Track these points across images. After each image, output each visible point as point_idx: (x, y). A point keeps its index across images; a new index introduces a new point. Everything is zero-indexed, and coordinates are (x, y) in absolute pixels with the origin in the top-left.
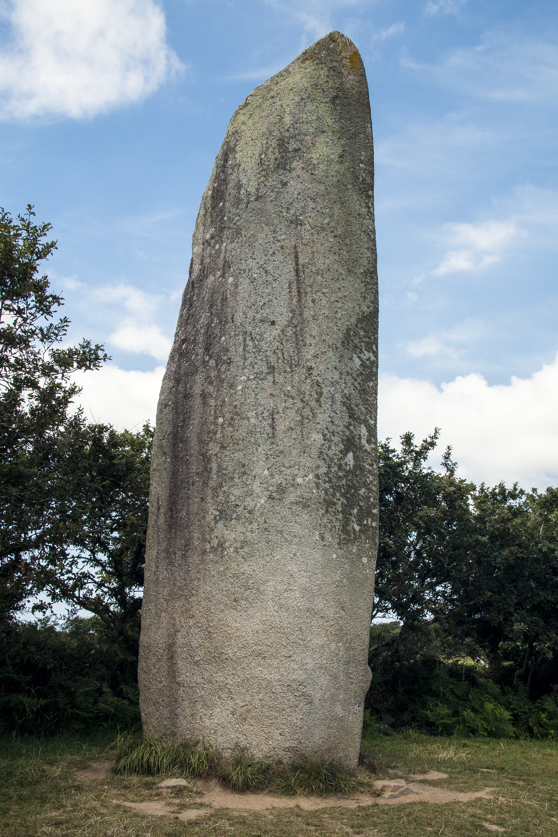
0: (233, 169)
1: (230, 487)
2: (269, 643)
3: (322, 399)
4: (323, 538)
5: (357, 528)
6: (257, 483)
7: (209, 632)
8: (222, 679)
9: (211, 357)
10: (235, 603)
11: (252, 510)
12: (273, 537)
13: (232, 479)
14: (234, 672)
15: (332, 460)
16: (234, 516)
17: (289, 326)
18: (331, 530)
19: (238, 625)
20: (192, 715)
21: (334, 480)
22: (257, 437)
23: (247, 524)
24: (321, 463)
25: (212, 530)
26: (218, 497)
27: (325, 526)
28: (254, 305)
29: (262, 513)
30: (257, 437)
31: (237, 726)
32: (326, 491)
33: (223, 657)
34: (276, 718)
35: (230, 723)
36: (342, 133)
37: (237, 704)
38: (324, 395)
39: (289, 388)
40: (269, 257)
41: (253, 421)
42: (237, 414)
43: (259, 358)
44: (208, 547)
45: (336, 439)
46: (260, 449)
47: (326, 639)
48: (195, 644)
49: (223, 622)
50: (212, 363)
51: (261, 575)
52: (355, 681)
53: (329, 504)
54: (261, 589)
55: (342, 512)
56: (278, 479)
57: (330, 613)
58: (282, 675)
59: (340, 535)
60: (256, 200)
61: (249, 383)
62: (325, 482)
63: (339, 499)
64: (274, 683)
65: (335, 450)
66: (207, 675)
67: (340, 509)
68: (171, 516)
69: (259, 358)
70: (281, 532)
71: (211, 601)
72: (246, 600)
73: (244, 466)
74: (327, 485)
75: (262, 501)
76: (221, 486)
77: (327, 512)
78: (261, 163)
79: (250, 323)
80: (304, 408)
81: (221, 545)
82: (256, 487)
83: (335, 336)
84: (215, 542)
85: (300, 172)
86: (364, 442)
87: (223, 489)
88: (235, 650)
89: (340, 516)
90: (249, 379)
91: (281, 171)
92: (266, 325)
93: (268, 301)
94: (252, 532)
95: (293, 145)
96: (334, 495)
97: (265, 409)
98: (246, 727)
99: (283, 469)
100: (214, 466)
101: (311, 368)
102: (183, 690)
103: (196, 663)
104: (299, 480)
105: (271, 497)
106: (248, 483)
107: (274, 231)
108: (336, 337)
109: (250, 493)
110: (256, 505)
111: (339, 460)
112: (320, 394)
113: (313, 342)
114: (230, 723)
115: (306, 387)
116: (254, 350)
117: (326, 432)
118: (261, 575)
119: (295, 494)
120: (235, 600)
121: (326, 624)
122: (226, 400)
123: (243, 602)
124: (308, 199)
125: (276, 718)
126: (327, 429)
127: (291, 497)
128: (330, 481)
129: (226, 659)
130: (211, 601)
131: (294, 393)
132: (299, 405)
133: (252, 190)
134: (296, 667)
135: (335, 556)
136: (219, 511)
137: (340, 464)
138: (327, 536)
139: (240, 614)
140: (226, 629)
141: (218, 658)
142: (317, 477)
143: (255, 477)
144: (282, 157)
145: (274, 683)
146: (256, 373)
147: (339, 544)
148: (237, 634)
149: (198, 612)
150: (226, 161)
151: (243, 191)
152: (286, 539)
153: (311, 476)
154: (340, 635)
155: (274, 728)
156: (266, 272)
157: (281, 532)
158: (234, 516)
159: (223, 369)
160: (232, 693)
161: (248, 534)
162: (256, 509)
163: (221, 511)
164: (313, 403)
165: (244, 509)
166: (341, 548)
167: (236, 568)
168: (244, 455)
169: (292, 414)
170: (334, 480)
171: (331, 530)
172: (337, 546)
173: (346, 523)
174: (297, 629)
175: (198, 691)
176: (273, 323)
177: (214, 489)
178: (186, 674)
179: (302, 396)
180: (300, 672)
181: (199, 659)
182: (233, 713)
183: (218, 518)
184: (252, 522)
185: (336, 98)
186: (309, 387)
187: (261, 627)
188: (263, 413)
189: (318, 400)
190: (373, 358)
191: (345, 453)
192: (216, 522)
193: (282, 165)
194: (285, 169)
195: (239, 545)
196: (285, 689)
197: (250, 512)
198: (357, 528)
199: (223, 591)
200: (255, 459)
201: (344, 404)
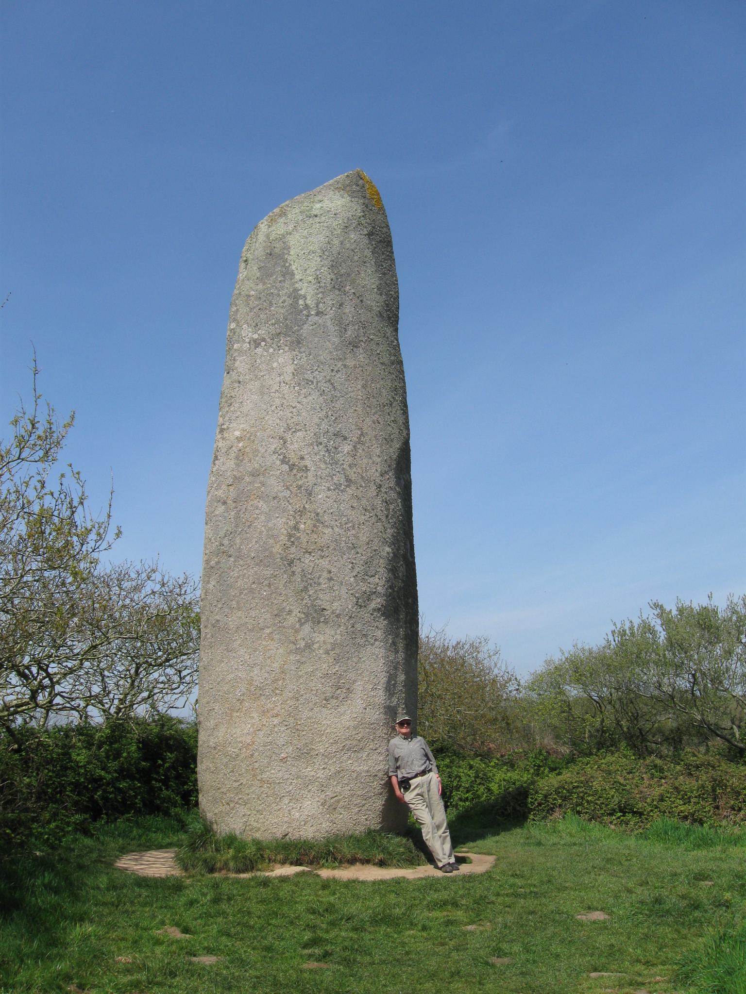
0: (284, 276)
8: (313, 773)
12: (362, 641)
33: (313, 753)
36: (378, 264)
60: (317, 314)
81: (308, 646)
91: (337, 292)
92: (339, 440)
99: (366, 577)
140: (316, 726)
158: (322, 619)
176: (345, 439)
183: (303, 621)
187: (352, 723)
192: (302, 624)
195: (329, 647)
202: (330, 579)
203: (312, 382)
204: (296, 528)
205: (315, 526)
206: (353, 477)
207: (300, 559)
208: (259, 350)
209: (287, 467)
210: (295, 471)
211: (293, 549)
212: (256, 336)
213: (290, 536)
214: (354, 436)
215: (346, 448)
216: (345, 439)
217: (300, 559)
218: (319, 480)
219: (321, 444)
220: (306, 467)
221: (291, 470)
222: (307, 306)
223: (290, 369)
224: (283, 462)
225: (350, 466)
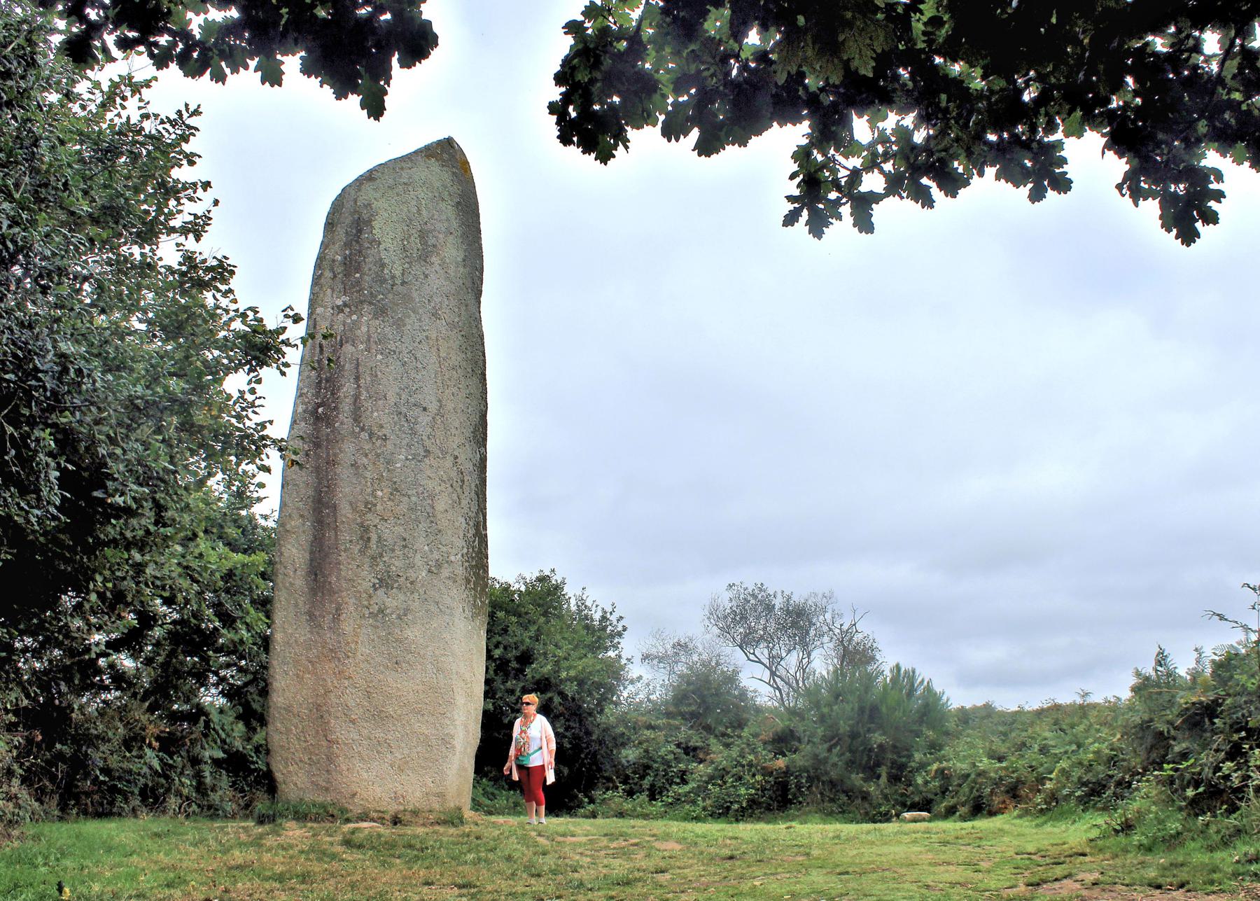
6: (418, 556)
9: (363, 429)
12: (433, 608)
13: (393, 550)
41: (413, 499)
42: (396, 489)
48: (351, 703)
50: (364, 435)
53: (468, 581)
56: (436, 555)
68: (315, 580)
70: (437, 603)
76: (381, 556)
78: (404, 249)
82: (418, 560)
84: (375, 609)
100: (374, 537)
101: (456, 458)
104: (452, 558)
107: (420, 320)
109: (412, 566)
112: (463, 481)
115: (454, 474)
127: (445, 572)
131: (445, 478)
133: (398, 273)
141: (379, 716)
150: (360, 231)
151: (386, 271)
157: (437, 603)
163: (381, 580)
176: (425, 409)
177: (373, 558)
178: (341, 731)
185: (458, 203)
187: (421, 687)
189: (461, 487)
192: (376, 589)
193: (424, 257)
197: (412, 583)
202: (405, 547)
204: (373, 494)
211: (369, 516)
213: (367, 503)
214: (433, 407)
215: (424, 419)
222: (393, 277)
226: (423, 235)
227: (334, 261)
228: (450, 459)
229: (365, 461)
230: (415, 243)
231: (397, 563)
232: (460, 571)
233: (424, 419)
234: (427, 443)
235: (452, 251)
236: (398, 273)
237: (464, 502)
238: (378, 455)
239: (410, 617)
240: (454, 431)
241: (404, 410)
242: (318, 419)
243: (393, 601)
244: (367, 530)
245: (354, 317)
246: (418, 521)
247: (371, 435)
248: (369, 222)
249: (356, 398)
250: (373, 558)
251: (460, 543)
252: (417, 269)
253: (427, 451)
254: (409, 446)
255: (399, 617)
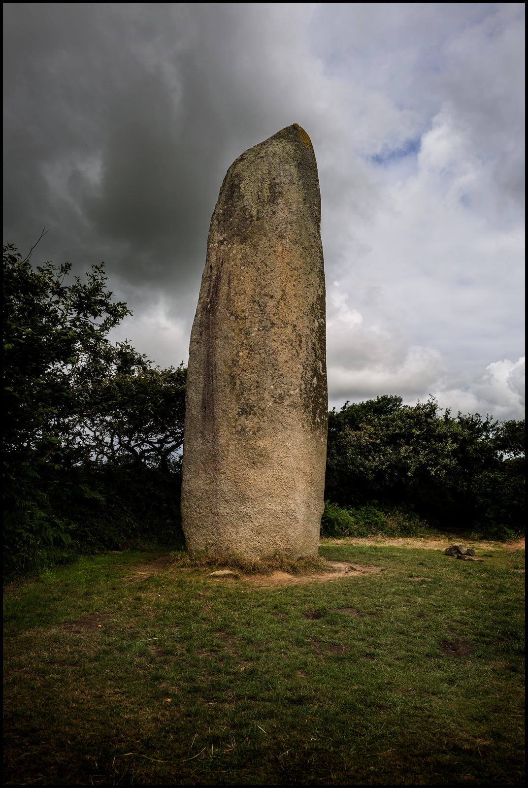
0: (238, 198)
1: (249, 395)
2: (275, 488)
3: (302, 345)
4: (303, 426)
5: (319, 421)
6: (267, 392)
7: (236, 482)
10: (253, 465)
11: (264, 409)
12: (278, 426)
14: (253, 506)
15: (307, 381)
16: (252, 412)
17: (282, 299)
18: (307, 422)
19: (255, 478)
20: (224, 532)
21: (308, 393)
22: (266, 365)
23: (260, 418)
24: (302, 382)
25: (236, 420)
26: (240, 400)
27: (304, 420)
28: (260, 285)
29: (270, 411)
30: (266, 365)
31: (255, 538)
32: (305, 398)
34: (279, 532)
35: (250, 536)
37: (254, 524)
38: (303, 342)
39: (284, 337)
40: (267, 256)
41: (263, 355)
42: (252, 350)
43: (265, 317)
44: (234, 430)
45: (309, 369)
46: (268, 373)
47: (305, 485)
48: (225, 489)
49: (245, 476)
51: (270, 448)
52: (318, 509)
54: (270, 456)
55: (313, 411)
56: (279, 391)
57: (307, 470)
58: (283, 507)
59: (312, 425)
60: (257, 220)
61: (259, 332)
62: (304, 394)
63: (311, 404)
64: (278, 511)
65: (309, 375)
66: (234, 508)
67: (311, 410)
69: (265, 317)
70: (281, 423)
71: (237, 464)
72: (261, 463)
73: (258, 382)
74: (305, 396)
75: (270, 404)
76: (243, 394)
77: (305, 411)
79: (257, 296)
80: (292, 349)
81: (243, 429)
82: (266, 395)
83: (306, 307)
85: (282, 206)
86: (321, 371)
87: (244, 396)
88: (254, 493)
89: (311, 414)
90: (259, 330)
91: (272, 204)
93: (269, 283)
94: (264, 422)
95: (279, 189)
96: (308, 401)
97: (270, 348)
98: (260, 538)
99: (282, 385)
100: (238, 382)
101: (295, 326)
102: (218, 518)
103: (227, 501)
104: (292, 392)
105: (275, 402)
106: (261, 393)
107: (270, 241)
108: (306, 309)
109: (262, 399)
110: (267, 406)
111: (310, 381)
113: (296, 310)
114: (250, 536)
115: (293, 337)
116: (261, 313)
117: (304, 364)
118: (270, 448)
119: (289, 400)
120: (253, 463)
121: (305, 477)
122: (244, 341)
123: (259, 464)
124: (288, 223)
125: (279, 532)
126: (305, 362)
127: (287, 402)
128: (306, 393)
129: (248, 498)
130: (237, 464)
131: (286, 340)
132: (290, 347)
133: (254, 213)
134: (291, 502)
135: (309, 437)
136: (241, 409)
137: (311, 383)
138: (305, 425)
139: (256, 471)
140: (248, 480)
141: (242, 498)
142: (301, 390)
143: (265, 389)
144: (272, 196)
145: (278, 511)
146: (264, 327)
147: (311, 430)
148: (255, 483)
149: (227, 470)
151: (247, 213)
152: (284, 427)
153: (298, 390)
154: (311, 483)
155: (277, 538)
156: (266, 265)
157: (281, 423)
159: (241, 322)
160: (251, 518)
161: (261, 423)
162: (267, 408)
163: (243, 409)
164: (297, 347)
165: (259, 408)
166: (312, 433)
167: (254, 443)
168: (258, 376)
169: (286, 352)
170: (308, 393)
171: (307, 422)
172: (310, 431)
173: (314, 419)
174: (292, 479)
175: (228, 518)
176: (272, 297)
177: (238, 396)
179: (291, 342)
180: (294, 505)
181: (229, 498)
182: (252, 530)
184: (264, 416)
186: (294, 337)
187: (270, 479)
188: (269, 351)
189: (300, 345)
190: (324, 322)
191: (313, 377)
192: (240, 416)
193: (273, 200)
194: (274, 203)
196: (285, 515)
197: (262, 410)
198: (319, 421)
199: (245, 457)
200: (265, 378)
201: (313, 348)
202: (258, 387)
203: (252, 263)
204: (237, 355)
205: (249, 353)
206: (276, 321)
207: (239, 375)
208: (223, 247)
209: (234, 317)
210: (238, 320)
212: (221, 238)
213: (233, 360)
214: (278, 295)
216: (272, 297)
217: (239, 375)
218: (253, 325)
219: (255, 301)
220: (245, 316)
221: (236, 319)
222: (251, 216)
223: (239, 256)
224: (232, 315)
225: (274, 315)
226: (272, 187)
227: (219, 214)
228: (289, 330)
229: (233, 334)
230: (266, 193)
231: (252, 398)
232: (299, 400)
233: (271, 303)
234: (273, 318)
235: (294, 195)
236: (254, 213)
237: (302, 355)
238: (240, 330)
239: (261, 433)
240: (293, 309)
241: (257, 299)
242: (208, 311)
243: (250, 423)
244: (234, 377)
245: (230, 246)
246: (266, 370)
247: (237, 317)
248: (238, 186)
249: (228, 295)
250: (238, 396)
251: (297, 382)
252: (268, 209)
253: (273, 324)
254: (261, 322)
255: (254, 433)
